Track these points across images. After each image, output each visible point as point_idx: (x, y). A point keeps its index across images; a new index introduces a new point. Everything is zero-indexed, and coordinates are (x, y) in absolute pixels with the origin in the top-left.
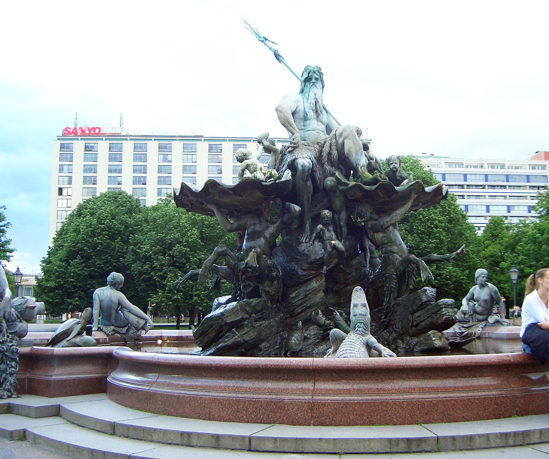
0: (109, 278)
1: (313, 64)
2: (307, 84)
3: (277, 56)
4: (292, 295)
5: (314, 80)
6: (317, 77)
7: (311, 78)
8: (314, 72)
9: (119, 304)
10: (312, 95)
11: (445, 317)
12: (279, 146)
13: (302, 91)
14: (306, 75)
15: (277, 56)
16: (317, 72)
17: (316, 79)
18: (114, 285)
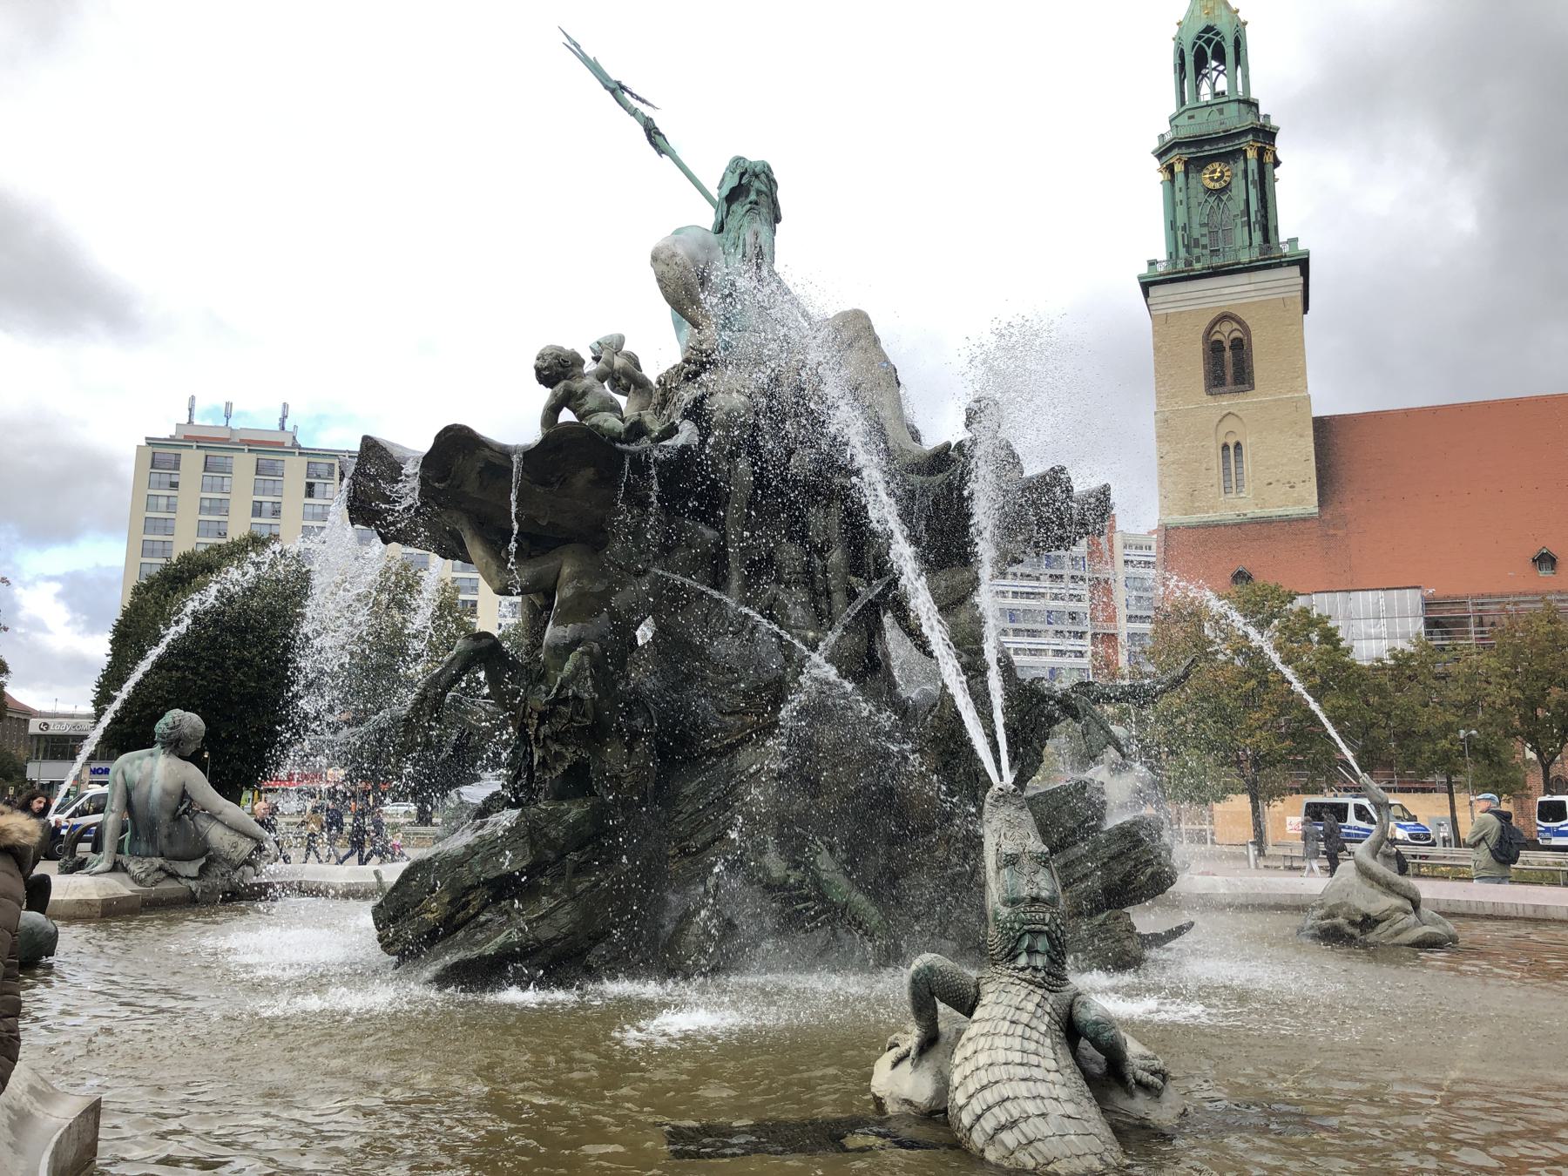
0: (161, 727)
1: (754, 155)
2: (739, 209)
3: (653, 134)
4: (689, 789)
5: (753, 197)
6: (764, 188)
7: (750, 193)
8: (757, 176)
9: (184, 795)
10: (750, 239)
11: (1149, 871)
12: (652, 370)
13: (720, 228)
14: (733, 182)
15: (653, 134)
16: (763, 177)
17: (759, 192)
18: (175, 745)
